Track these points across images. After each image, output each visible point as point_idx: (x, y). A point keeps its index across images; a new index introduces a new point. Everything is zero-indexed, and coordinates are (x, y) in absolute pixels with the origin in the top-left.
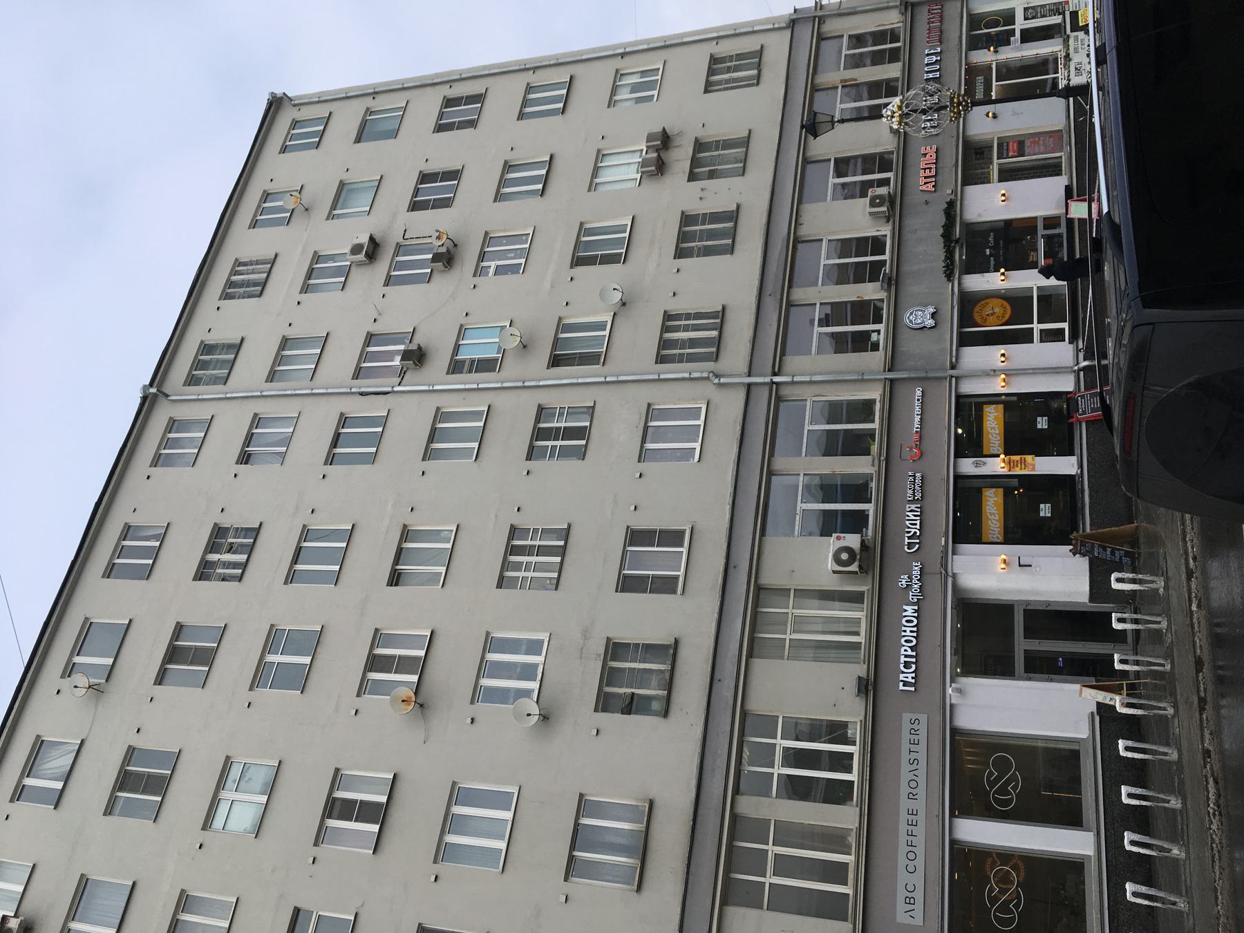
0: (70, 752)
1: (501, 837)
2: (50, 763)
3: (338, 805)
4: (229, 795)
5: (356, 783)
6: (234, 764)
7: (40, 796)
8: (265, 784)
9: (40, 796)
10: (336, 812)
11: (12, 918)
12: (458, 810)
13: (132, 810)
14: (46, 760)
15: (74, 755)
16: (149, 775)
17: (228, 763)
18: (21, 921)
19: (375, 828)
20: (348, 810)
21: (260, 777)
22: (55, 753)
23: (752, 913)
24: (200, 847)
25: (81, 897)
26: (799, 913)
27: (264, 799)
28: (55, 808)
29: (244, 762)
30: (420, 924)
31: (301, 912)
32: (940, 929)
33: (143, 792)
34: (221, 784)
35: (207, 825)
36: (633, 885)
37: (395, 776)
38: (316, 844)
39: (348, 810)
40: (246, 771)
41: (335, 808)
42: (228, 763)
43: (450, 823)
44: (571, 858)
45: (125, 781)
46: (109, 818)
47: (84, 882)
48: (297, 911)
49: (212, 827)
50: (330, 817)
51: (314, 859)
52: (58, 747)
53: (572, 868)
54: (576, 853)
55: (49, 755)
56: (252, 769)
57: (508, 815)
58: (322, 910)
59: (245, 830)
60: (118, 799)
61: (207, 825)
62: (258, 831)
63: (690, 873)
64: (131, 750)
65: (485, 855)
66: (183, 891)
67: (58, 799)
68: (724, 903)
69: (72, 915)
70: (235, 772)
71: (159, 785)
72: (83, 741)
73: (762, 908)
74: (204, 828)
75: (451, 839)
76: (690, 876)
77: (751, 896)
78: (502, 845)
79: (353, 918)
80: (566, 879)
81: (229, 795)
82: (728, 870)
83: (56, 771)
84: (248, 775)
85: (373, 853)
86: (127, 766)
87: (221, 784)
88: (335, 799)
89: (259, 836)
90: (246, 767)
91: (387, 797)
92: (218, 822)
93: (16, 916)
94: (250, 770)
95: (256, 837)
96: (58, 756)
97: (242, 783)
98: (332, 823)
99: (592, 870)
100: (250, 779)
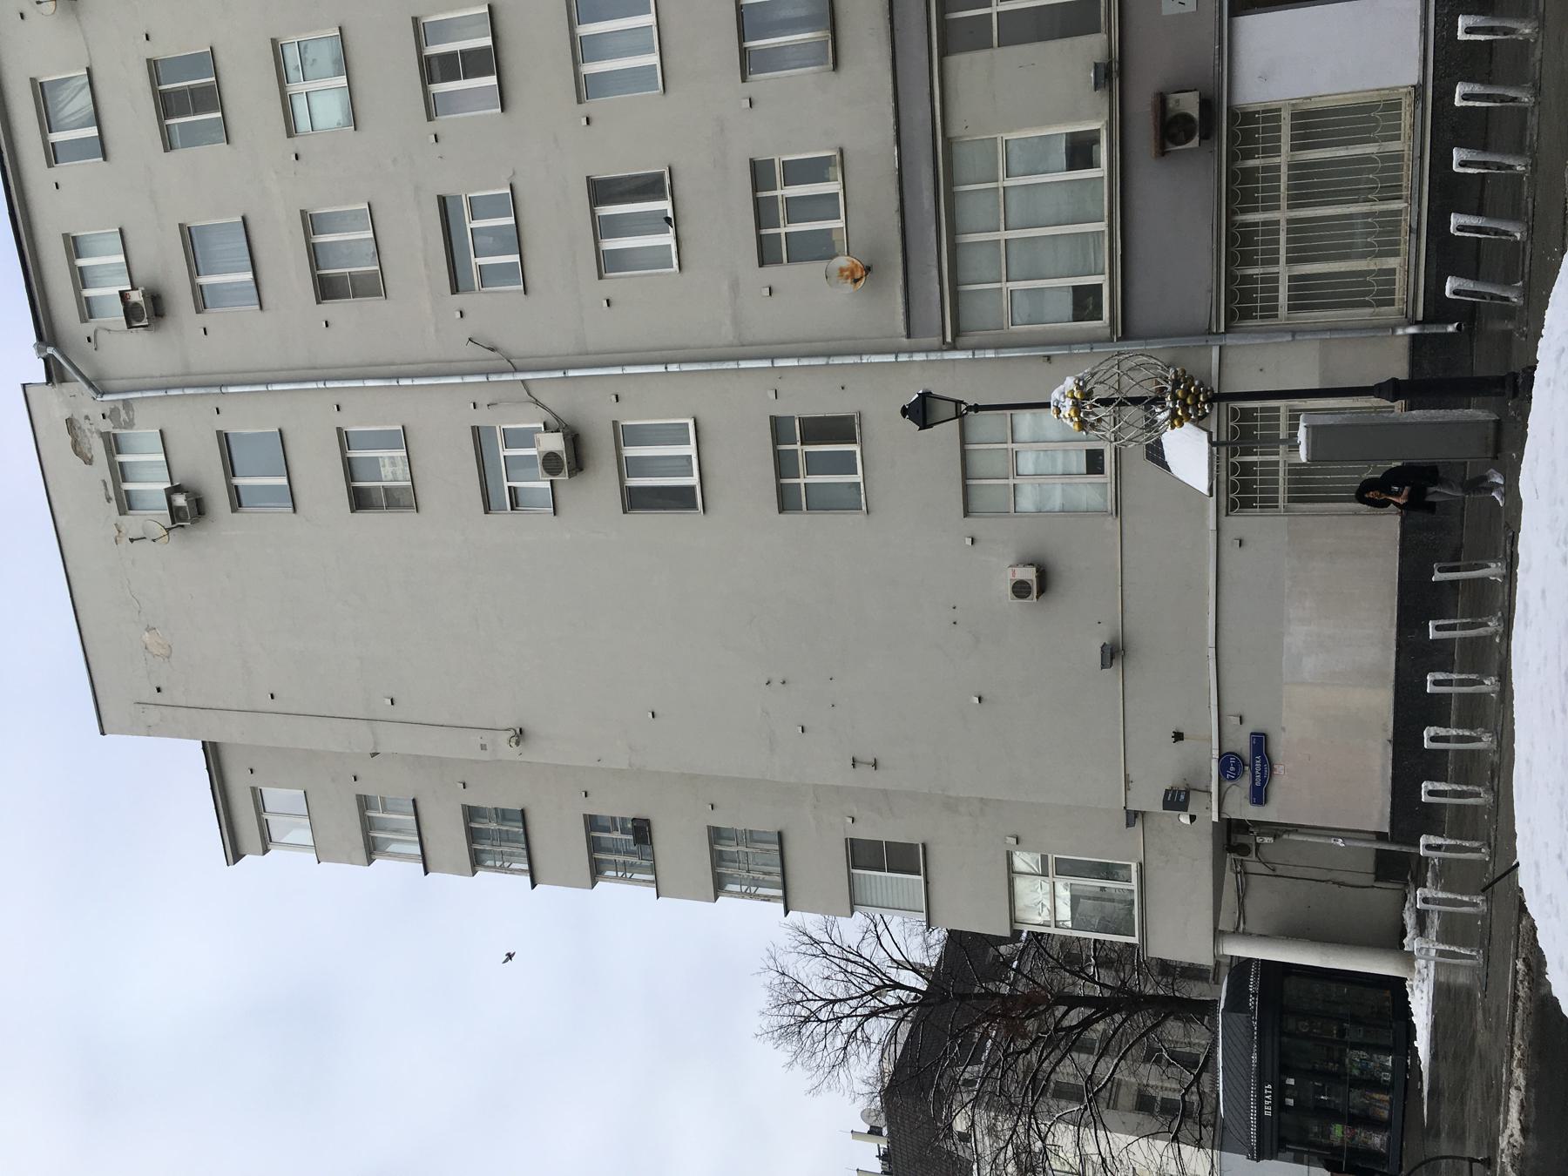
0: (80, 90)
1: (650, 50)
2: (68, 107)
3: (435, 64)
4: (301, 87)
5: (445, 30)
6: (284, 47)
7: (79, 149)
8: (336, 62)
9: (79, 149)
10: (437, 73)
11: (131, 293)
12: (585, 30)
13: (193, 137)
14: (61, 106)
15: (88, 88)
16: (192, 90)
17: (277, 49)
18: (143, 292)
19: (492, 80)
20: (450, 67)
21: (325, 55)
22: (64, 94)
23: (981, 56)
24: (297, 158)
25: (193, 247)
26: (1041, 39)
27: (343, 81)
28: (105, 159)
29: (296, 41)
30: (588, 177)
31: (447, 200)
32: (1217, 9)
33: (196, 113)
34: (282, 78)
35: (291, 130)
36: (827, 64)
37: (490, 7)
38: (430, 119)
39: (450, 67)
40: (305, 52)
41: (434, 69)
42: (277, 49)
43: (580, 50)
44: (743, 52)
45: (167, 105)
46: (172, 154)
47: (188, 235)
48: (442, 201)
49: (298, 130)
50: (432, 81)
51: (436, 136)
52: (65, 86)
53: (747, 63)
54: (748, 44)
55: (60, 99)
56: (310, 45)
57: (649, 20)
58: (472, 192)
59: (339, 124)
60: (172, 129)
61: (291, 130)
62: (355, 121)
63: (895, 28)
64: (153, 65)
65: (637, 78)
66: (303, 212)
67: (101, 148)
68: (943, 54)
69: (194, 269)
70: (292, 56)
71: (209, 98)
72: (88, 69)
73: (992, 47)
74: (290, 135)
75: (589, 68)
76: (896, 32)
77: (977, 37)
78: (654, 59)
79: (509, 191)
80: (744, 80)
81: (301, 87)
82: (943, 9)
83: (81, 115)
84: (309, 56)
85: (502, 111)
86: (159, 85)
87: (282, 78)
88: (429, 58)
89: (358, 128)
90: (302, 48)
91: (490, 38)
92: (303, 123)
93: (134, 288)
94: (308, 50)
95: (355, 129)
96: (70, 98)
97: (308, 68)
98: (438, 88)
99: (774, 60)
100: (314, 60)
